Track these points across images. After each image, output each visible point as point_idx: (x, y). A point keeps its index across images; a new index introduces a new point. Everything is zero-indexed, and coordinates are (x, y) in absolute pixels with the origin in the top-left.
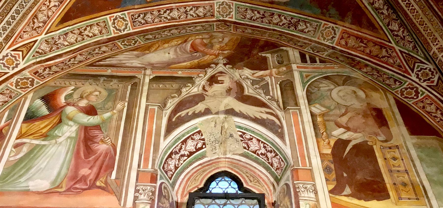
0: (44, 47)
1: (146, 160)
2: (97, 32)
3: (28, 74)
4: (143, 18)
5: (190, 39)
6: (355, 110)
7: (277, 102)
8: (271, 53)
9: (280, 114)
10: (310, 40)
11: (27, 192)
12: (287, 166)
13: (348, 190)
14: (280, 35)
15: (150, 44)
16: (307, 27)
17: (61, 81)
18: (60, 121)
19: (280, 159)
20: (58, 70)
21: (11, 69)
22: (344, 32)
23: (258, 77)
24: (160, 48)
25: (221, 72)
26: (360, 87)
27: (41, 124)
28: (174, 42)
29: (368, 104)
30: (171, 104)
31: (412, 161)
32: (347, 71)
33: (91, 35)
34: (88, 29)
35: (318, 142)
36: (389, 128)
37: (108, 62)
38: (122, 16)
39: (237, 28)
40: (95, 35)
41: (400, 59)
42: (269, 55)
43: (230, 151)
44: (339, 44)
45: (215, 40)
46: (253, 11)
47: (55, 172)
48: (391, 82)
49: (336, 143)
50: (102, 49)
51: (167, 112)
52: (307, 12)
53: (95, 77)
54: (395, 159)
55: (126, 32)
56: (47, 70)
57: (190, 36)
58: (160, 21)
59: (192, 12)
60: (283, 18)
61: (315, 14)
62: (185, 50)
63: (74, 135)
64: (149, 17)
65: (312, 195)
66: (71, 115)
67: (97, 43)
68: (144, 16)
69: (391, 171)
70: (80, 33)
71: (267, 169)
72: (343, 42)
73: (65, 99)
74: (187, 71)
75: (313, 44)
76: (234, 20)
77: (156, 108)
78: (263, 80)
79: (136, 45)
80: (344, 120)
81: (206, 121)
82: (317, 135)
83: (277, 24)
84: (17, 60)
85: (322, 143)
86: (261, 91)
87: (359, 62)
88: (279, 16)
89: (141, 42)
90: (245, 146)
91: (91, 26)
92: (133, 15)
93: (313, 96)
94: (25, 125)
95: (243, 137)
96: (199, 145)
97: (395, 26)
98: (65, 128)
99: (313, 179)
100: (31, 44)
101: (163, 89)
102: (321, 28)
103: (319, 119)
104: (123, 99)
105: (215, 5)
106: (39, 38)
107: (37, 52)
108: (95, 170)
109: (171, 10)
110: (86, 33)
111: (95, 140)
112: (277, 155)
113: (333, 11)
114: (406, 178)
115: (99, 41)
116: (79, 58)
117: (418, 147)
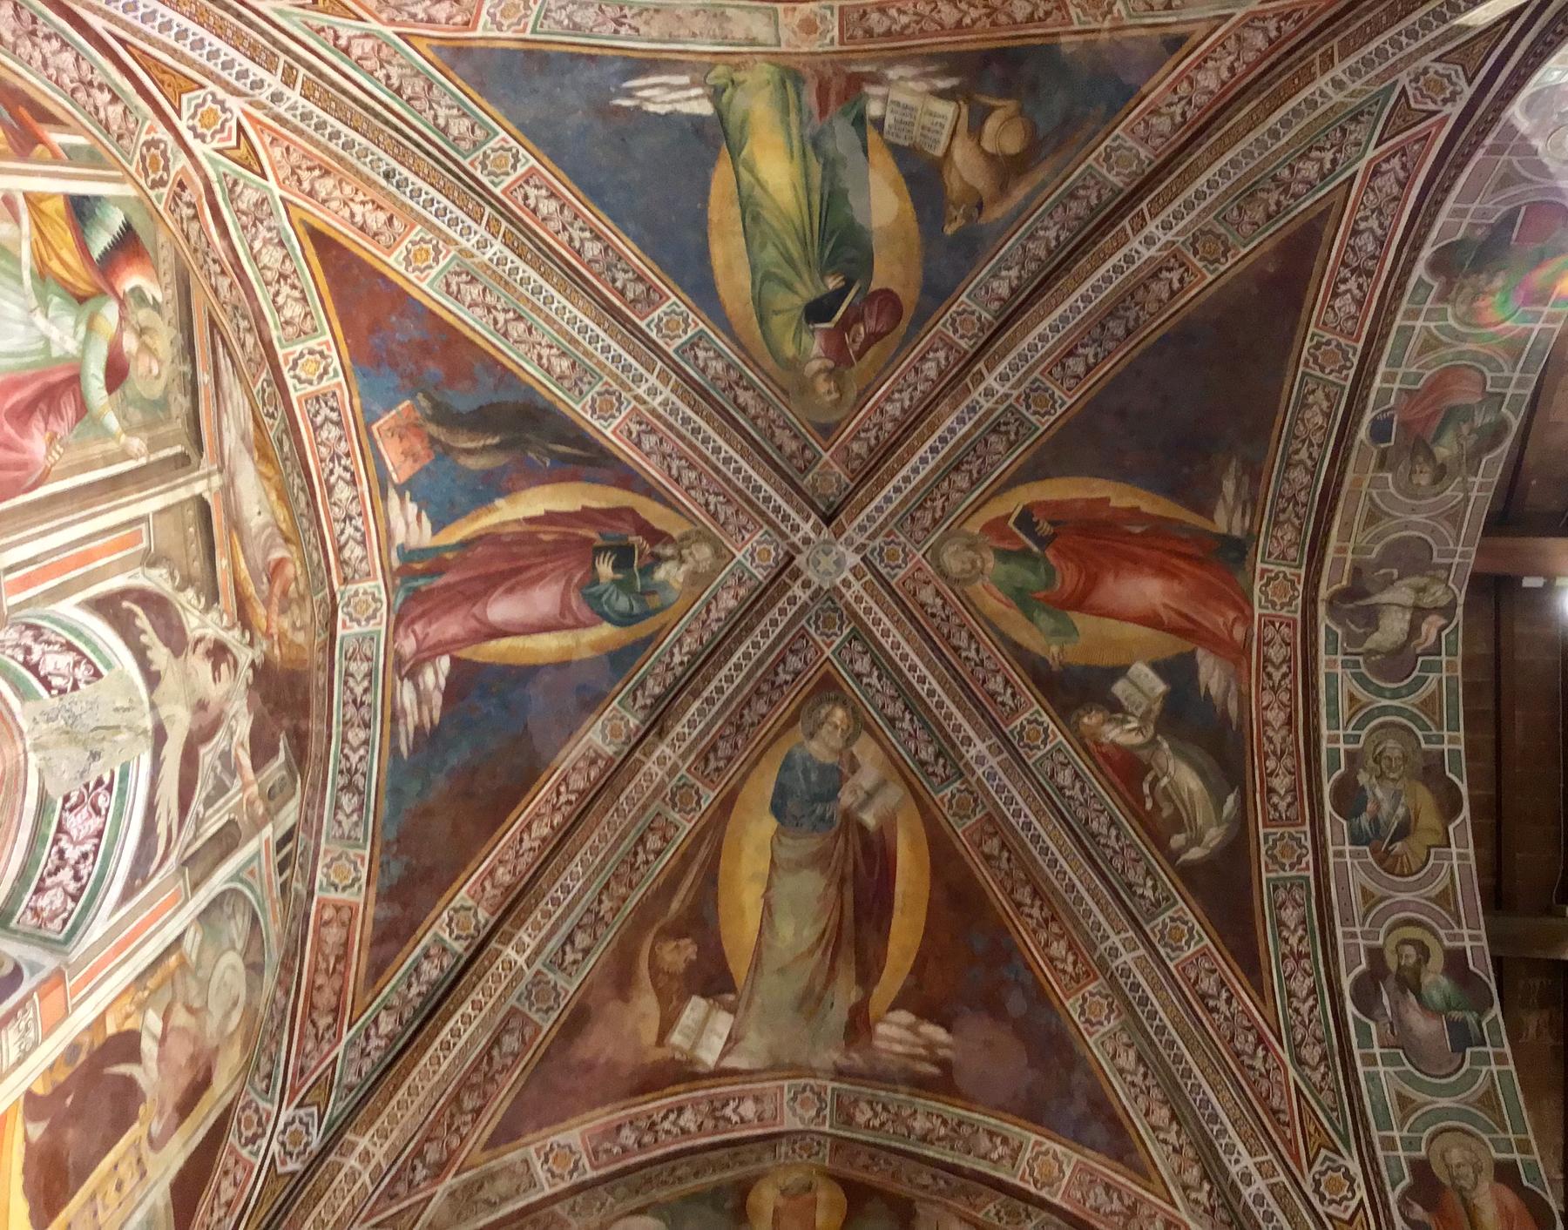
0: (249, 197)
1: (26, 583)
2: (288, 313)
3: (178, 167)
4: (327, 419)
5: (293, 548)
6: (202, 1028)
7: (195, 838)
8: (287, 761)
10: (319, 832)
12: (58, 942)
15: (271, 453)
16: (348, 816)
17: (171, 259)
18: (82, 300)
19: (65, 915)
20: (193, 240)
21: (191, 123)
22: (352, 909)
24: (266, 483)
26: (248, 1004)
27: (71, 251)
28: (282, 513)
30: (157, 580)
32: (273, 956)
33: (280, 300)
34: (297, 294)
35: (126, 991)
37: (224, 363)
38: (331, 370)
40: (279, 310)
41: (320, 1063)
43: (47, 760)
46: (369, 675)
48: (265, 1067)
50: (248, 336)
52: (385, 805)
53: (189, 349)
55: (290, 382)
56: (190, 212)
58: (322, 460)
59: (349, 531)
60: (362, 752)
61: (384, 827)
62: (271, 547)
63: (56, 352)
66: (99, 321)
68: (332, 422)
69: (93, 1197)
70: (283, 276)
71: (23, 876)
73: (133, 290)
74: (230, 578)
76: (340, 632)
77: (144, 545)
79: (266, 420)
81: (132, 687)
83: (345, 741)
84: (213, 136)
85: (127, 1000)
88: (366, 742)
90: (74, 800)
91: (304, 299)
92: (334, 394)
93: (215, 913)
94: (60, 204)
95: (96, 788)
96: (56, 681)
97: (387, 1024)
100: (256, 168)
101: (186, 539)
102: (352, 853)
105: (372, 583)
106: (272, 183)
107: (235, 183)
109: (353, 483)
110: (285, 290)
111: (51, 419)
112: (75, 899)
113: (396, 869)
115: (264, 319)
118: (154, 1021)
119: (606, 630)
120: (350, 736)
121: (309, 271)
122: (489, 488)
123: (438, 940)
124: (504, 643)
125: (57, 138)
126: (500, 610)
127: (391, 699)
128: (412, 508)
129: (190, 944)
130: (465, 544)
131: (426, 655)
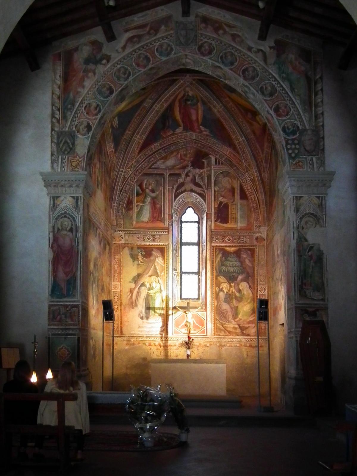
1: (170, 211)
7: (205, 185)
8: (206, 159)
9: (206, 191)
11: (143, 222)
13: (219, 221)
14: (210, 148)
23: (200, 173)
25: (189, 171)
28: (175, 154)
29: (232, 186)
30: (175, 187)
31: (238, 210)
36: (235, 196)
39: (195, 143)
42: (205, 161)
44: (228, 154)
45: (188, 152)
47: (148, 215)
49: (219, 203)
51: (174, 191)
54: (233, 209)
57: (180, 149)
64: (165, 142)
65: (210, 222)
67: (150, 155)
69: (231, 213)
72: (230, 154)
73: (145, 186)
75: (221, 152)
76: (194, 138)
77: (171, 189)
78: (202, 174)
80: (223, 193)
82: (215, 200)
86: (201, 180)
87: (234, 164)
89: (164, 155)
94: (137, 197)
98: (147, 198)
99: (211, 217)
103: (216, 193)
104: (161, 185)
108: (158, 215)
109: (173, 138)
114: (234, 216)
116: (146, 164)
117: (241, 204)
118: (221, 199)
119: (199, 104)
120: (209, 142)
121: (144, 152)
122: (175, 120)
123: (238, 143)
124: (199, 119)
125: (131, 197)
126: (194, 118)
127: (204, 135)
128: (177, 130)
129: (216, 189)
130: (183, 122)
131: (200, 129)
